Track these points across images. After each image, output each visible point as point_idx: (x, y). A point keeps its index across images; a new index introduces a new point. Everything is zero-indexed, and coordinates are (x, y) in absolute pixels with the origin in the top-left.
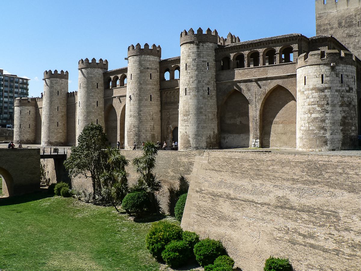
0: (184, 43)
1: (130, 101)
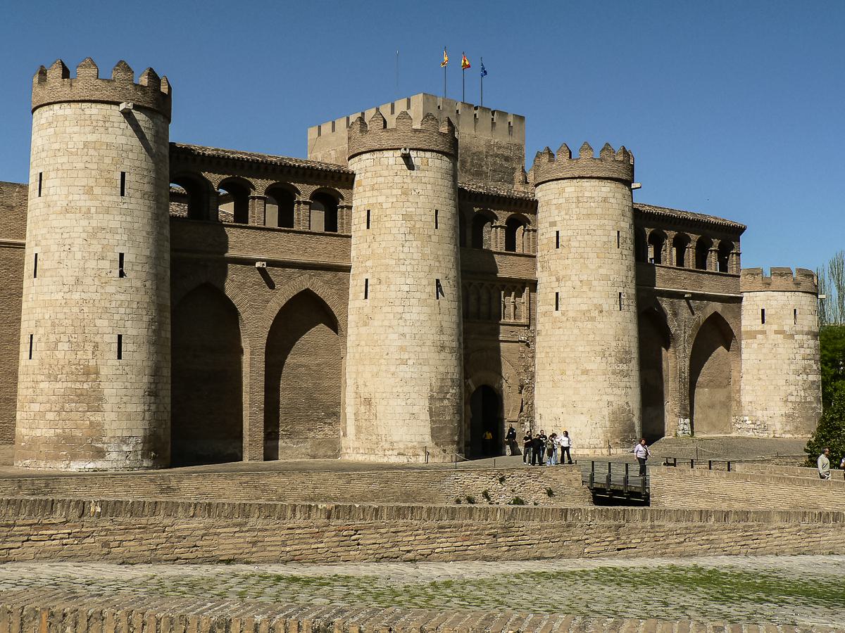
0: (614, 176)
1: (438, 298)
